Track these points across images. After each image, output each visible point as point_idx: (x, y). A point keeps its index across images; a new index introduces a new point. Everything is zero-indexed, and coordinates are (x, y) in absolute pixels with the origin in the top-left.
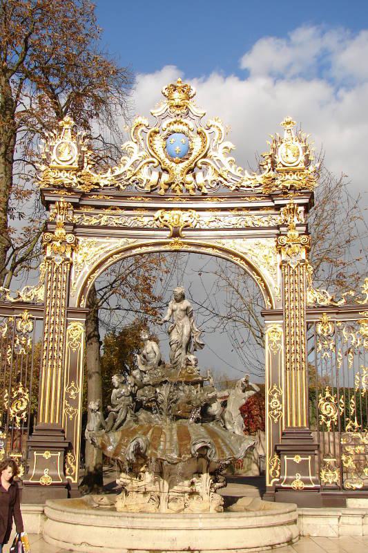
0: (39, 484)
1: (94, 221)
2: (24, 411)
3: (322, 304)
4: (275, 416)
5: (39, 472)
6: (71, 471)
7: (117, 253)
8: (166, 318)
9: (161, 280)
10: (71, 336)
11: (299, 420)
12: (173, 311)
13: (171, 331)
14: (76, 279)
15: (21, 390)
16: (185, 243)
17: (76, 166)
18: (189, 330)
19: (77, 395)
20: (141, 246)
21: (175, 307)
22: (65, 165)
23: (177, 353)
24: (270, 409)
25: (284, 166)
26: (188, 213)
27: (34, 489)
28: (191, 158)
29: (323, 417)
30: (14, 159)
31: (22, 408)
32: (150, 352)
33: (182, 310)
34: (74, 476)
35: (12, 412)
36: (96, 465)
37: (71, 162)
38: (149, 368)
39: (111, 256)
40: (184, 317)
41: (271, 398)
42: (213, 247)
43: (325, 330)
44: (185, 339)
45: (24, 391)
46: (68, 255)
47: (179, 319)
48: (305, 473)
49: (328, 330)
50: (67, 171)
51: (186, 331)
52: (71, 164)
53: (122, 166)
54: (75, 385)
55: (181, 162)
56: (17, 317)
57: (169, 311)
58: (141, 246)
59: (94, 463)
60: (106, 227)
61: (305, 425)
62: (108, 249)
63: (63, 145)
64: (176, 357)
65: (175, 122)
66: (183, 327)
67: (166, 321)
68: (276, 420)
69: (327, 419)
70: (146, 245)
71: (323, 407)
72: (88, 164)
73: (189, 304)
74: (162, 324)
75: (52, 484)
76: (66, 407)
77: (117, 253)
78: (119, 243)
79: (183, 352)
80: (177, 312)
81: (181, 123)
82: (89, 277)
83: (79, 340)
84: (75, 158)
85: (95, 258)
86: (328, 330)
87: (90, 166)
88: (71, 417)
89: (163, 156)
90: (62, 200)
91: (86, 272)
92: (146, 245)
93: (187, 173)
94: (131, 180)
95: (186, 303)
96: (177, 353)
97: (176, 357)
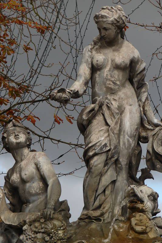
8: (77, 86)
9: (27, 49)
12: (95, 69)
13: (90, 122)
18: (137, 120)
21: (99, 58)
23: (106, 180)
32: (31, 179)
33: (117, 67)
38: (28, 218)
40: (123, 85)
47: (112, 91)
57: (84, 70)
64: (100, 191)
66: (121, 110)
67: (76, 95)
73: (136, 54)
74: (65, 102)
79: (122, 179)
80: (106, 72)
96: (106, 180)
97: (100, 191)
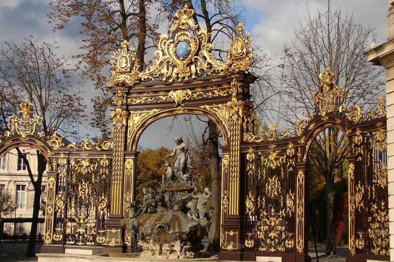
0: (109, 246)
1: (138, 101)
2: (105, 207)
3: (250, 141)
4: (225, 209)
5: (110, 240)
6: (127, 239)
7: (151, 118)
10: (127, 167)
11: (234, 211)
14: (130, 135)
15: (103, 197)
16: (185, 109)
17: (128, 70)
19: (130, 198)
20: (163, 113)
22: (123, 70)
23: (179, 174)
24: (223, 205)
25: (235, 56)
26: (185, 91)
27: (107, 248)
28: (190, 56)
29: (248, 210)
30: (145, 47)
31: (104, 207)
33: (180, 149)
34: (129, 242)
35: (99, 209)
36: (215, 238)
37: (126, 68)
39: (148, 120)
41: (224, 198)
42: (199, 110)
43: (251, 157)
44: (182, 166)
45: (105, 197)
46: (124, 123)
48: (235, 242)
49: (252, 157)
50: (125, 73)
51: (182, 161)
52: (126, 69)
53: (154, 66)
54: (129, 193)
55: (183, 60)
56: (101, 159)
58: (163, 113)
59: (213, 237)
60: (144, 104)
61: (237, 214)
62: (145, 117)
63: (122, 58)
65: (182, 34)
68: (225, 211)
69: (250, 210)
70: (166, 112)
71: (247, 203)
72: (136, 67)
75: (115, 246)
76: (125, 205)
77: (151, 118)
78: (152, 112)
81: (185, 34)
82: (136, 133)
83: (131, 169)
84: (129, 65)
85: (139, 123)
86: (252, 157)
87: (138, 68)
88: (127, 210)
89: (174, 57)
90: (119, 92)
91: (135, 130)
92: (166, 112)
93: (187, 66)
94: (158, 74)
95: (183, 145)
